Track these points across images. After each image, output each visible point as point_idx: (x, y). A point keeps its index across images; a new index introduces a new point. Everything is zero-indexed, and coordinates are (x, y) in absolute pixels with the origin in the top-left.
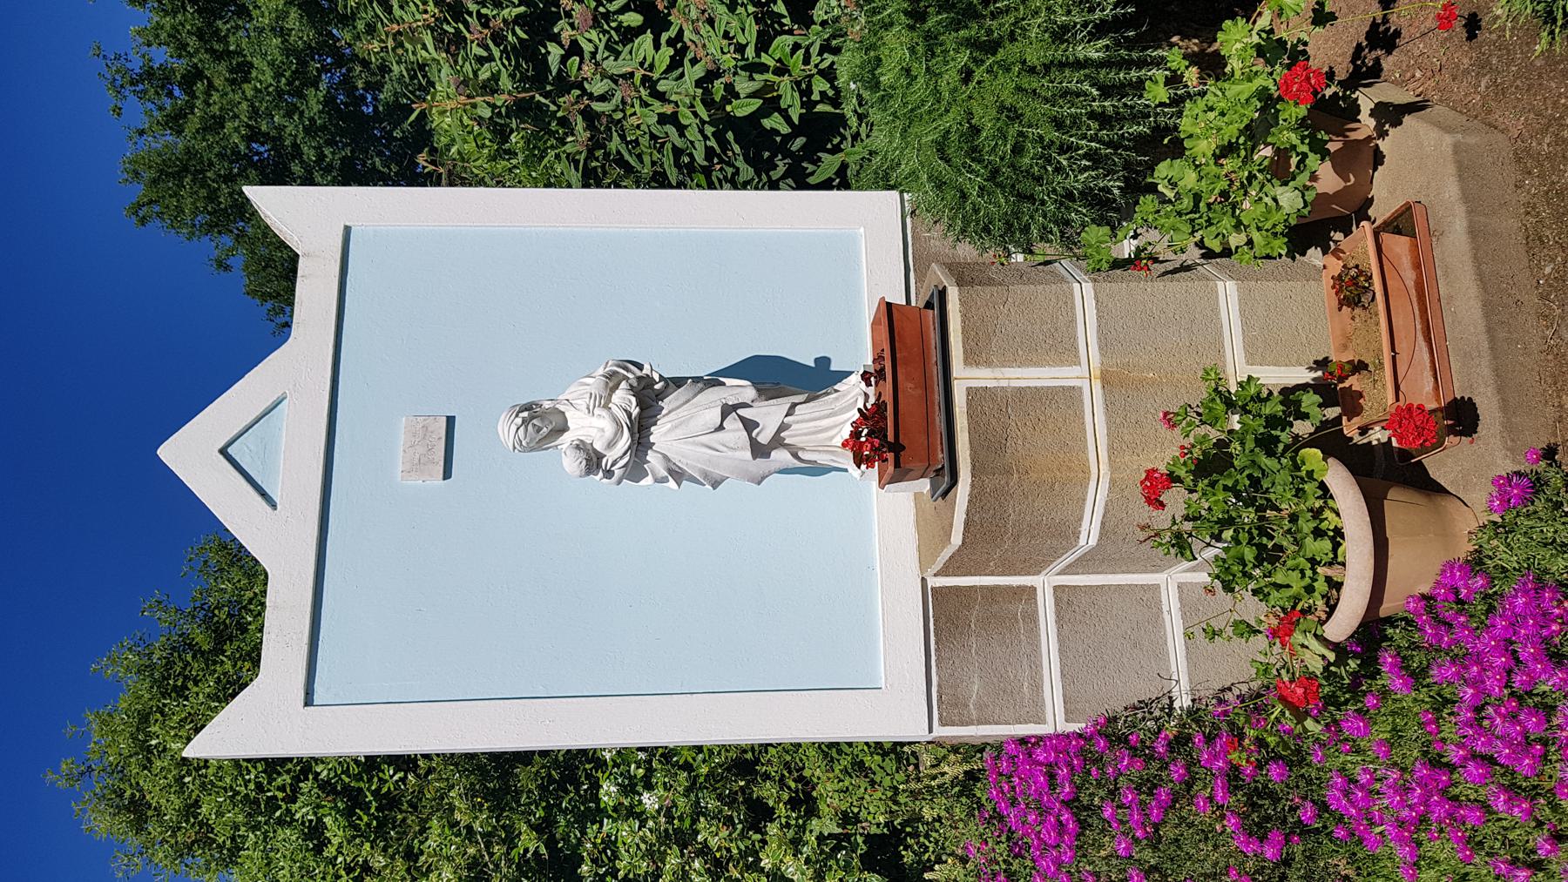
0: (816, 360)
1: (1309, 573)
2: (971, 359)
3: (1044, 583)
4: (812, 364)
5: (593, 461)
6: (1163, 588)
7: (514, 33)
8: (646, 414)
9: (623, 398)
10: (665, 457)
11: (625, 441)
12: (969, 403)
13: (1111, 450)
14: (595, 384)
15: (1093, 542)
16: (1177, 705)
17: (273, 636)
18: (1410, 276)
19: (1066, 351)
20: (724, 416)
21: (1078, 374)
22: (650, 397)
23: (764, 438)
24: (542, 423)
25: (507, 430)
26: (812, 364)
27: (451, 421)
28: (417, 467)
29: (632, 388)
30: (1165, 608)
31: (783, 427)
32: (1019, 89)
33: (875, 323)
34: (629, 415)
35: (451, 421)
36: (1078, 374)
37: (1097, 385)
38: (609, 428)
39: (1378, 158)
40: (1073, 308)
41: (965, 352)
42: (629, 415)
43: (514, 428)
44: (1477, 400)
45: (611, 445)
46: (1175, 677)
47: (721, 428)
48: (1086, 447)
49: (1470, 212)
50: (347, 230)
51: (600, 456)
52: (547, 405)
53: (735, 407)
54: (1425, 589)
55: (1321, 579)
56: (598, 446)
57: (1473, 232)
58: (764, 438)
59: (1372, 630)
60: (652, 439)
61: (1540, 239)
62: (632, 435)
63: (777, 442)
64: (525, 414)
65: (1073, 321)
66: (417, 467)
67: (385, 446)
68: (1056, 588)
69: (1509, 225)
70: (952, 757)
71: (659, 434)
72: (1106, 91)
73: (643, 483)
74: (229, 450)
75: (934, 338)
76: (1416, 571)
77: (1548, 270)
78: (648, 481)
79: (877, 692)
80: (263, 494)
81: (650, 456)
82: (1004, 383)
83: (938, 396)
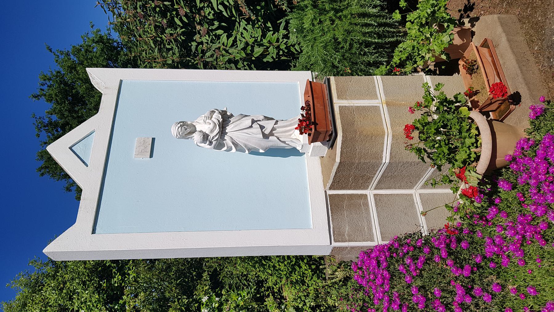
1: (468, 151)
2: (339, 97)
3: (370, 193)
5: (205, 137)
6: (414, 195)
7: (181, 38)
8: (224, 123)
10: (231, 137)
11: (217, 130)
12: (340, 111)
13: (391, 124)
14: (207, 114)
15: (388, 161)
16: (423, 235)
17: (82, 209)
18: (490, 59)
19: (374, 96)
20: (252, 124)
21: (379, 101)
22: (226, 119)
23: (267, 132)
25: (174, 130)
27: (153, 139)
28: (141, 153)
30: (415, 202)
32: (351, 23)
33: (306, 93)
34: (219, 121)
35: (153, 139)
36: (379, 101)
37: (385, 106)
39: (473, 34)
40: (374, 83)
41: (338, 95)
42: (219, 121)
43: (177, 128)
44: (519, 91)
46: (422, 225)
47: (251, 127)
48: (383, 124)
49: (506, 35)
50: (121, 81)
52: (189, 123)
53: (256, 121)
54: (511, 153)
55: (473, 153)
56: (207, 132)
57: (509, 40)
58: (267, 132)
59: (493, 173)
60: (227, 131)
61: (532, 41)
62: (220, 128)
63: (271, 134)
65: (375, 86)
66: (141, 153)
67: (129, 147)
68: (374, 195)
69: (521, 39)
70: (339, 270)
71: (229, 129)
72: (380, 25)
74: (73, 148)
75: (326, 92)
76: (507, 148)
77: (536, 48)
79: (312, 235)
80: (84, 162)
82: (352, 105)
83: (329, 109)
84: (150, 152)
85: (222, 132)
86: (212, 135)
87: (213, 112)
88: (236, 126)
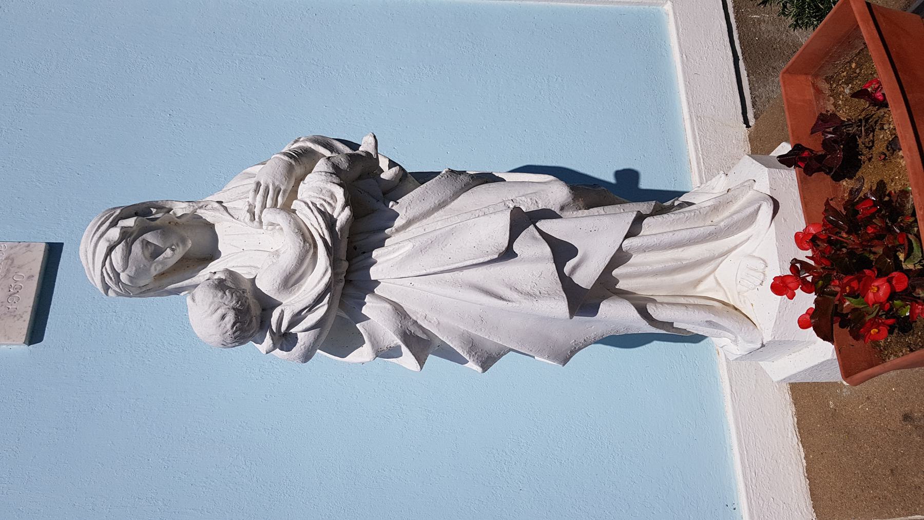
0: (618, 174)
4: (612, 180)
5: (251, 314)
9: (320, 190)
10: (399, 311)
11: (319, 275)
14: (268, 171)
20: (514, 233)
22: (371, 195)
24: (165, 243)
26: (612, 180)
29: (337, 171)
31: (620, 258)
34: (330, 222)
38: (287, 247)
42: (330, 222)
43: (103, 247)
45: (290, 281)
47: (508, 254)
51: (267, 305)
52: (180, 209)
56: (267, 286)
58: (586, 275)
62: (334, 263)
63: (606, 286)
64: (130, 222)
71: (388, 264)
73: (355, 357)
78: (363, 354)
81: (371, 307)
84: (27, 317)
85: (351, 278)
86: (290, 304)
87: (301, 161)
88: (423, 250)
